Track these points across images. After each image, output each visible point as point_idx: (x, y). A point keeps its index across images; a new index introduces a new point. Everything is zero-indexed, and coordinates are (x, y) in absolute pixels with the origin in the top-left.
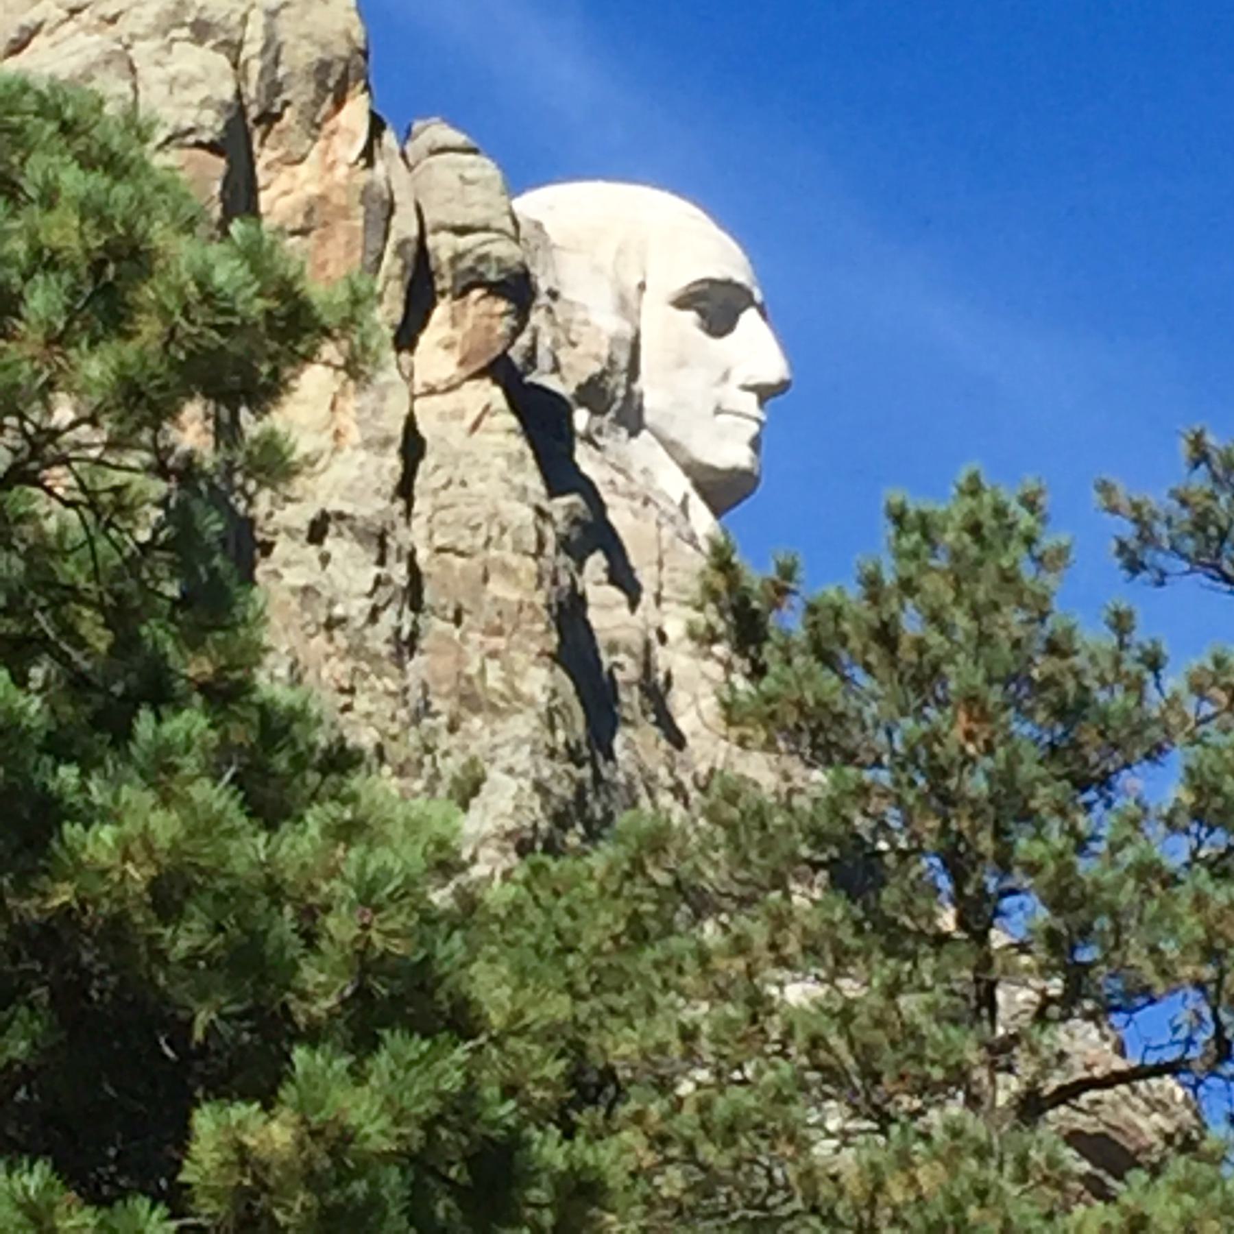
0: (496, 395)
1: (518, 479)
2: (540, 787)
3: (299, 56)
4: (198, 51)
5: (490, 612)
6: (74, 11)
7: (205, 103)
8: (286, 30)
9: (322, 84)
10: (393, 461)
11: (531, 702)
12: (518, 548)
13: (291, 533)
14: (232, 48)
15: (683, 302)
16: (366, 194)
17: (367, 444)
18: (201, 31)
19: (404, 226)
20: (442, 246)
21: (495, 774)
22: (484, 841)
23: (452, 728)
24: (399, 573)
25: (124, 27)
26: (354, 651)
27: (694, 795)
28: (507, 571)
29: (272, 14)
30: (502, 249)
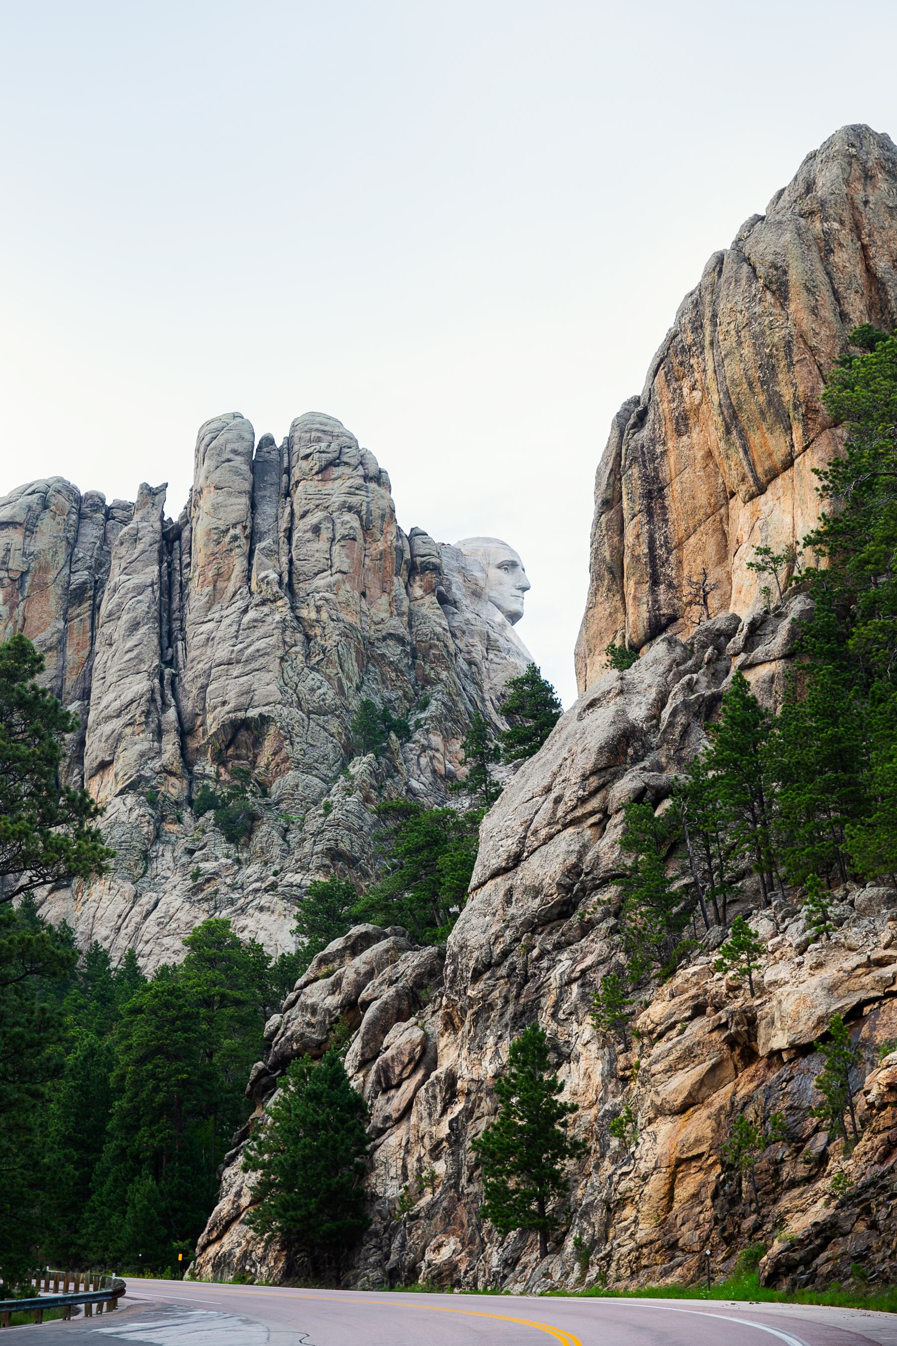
0: (434, 599)
1: (438, 620)
2: (443, 703)
3: (376, 513)
4: (351, 514)
5: (432, 657)
6: (317, 506)
7: (351, 528)
8: (373, 507)
9: (383, 520)
10: (405, 619)
11: (442, 680)
12: (438, 640)
13: (378, 639)
14: (358, 513)
15: (500, 567)
16: (396, 548)
17: (398, 615)
18: (350, 509)
19: (407, 556)
20: (419, 560)
21: (433, 702)
22: (426, 719)
23: (423, 688)
24: (408, 649)
25: (330, 510)
26: (396, 670)
27: (495, 701)
28: (436, 646)
29: (368, 503)
30: (433, 560)
